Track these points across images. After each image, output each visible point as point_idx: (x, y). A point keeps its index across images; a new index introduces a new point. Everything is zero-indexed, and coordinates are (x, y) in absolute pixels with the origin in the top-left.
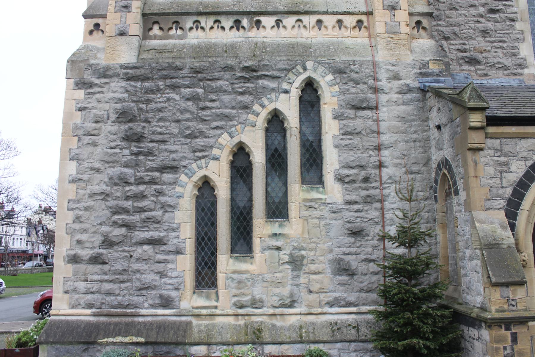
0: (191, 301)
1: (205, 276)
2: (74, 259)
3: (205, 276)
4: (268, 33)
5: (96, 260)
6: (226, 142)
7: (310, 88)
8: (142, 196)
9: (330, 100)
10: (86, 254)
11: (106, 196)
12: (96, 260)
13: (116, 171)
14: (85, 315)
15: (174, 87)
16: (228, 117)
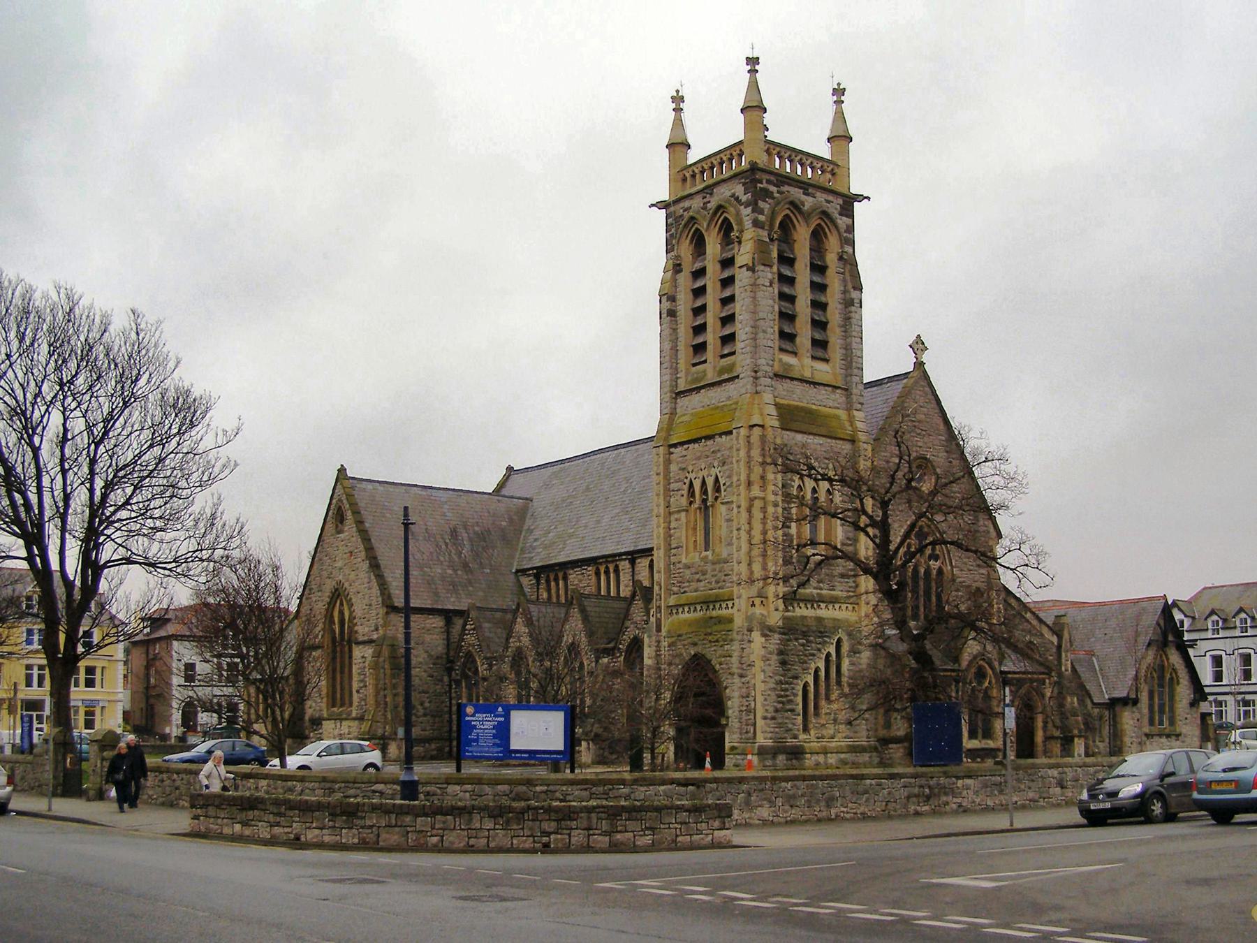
0: (802, 737)
1: (806, 729)
2: (765, 718)
3: (806, 729)
4: (825, 612)
5: (773, 718)
6: (813, 666)
7: (839, 642)
8: (786, 690)
9: (845, 648)
10: (769, 715)
11: (775, 689)
12: (773, 718)
13: (777, 678)
14: (769, 743)
15: (796, 639)
16: (813, 655)
